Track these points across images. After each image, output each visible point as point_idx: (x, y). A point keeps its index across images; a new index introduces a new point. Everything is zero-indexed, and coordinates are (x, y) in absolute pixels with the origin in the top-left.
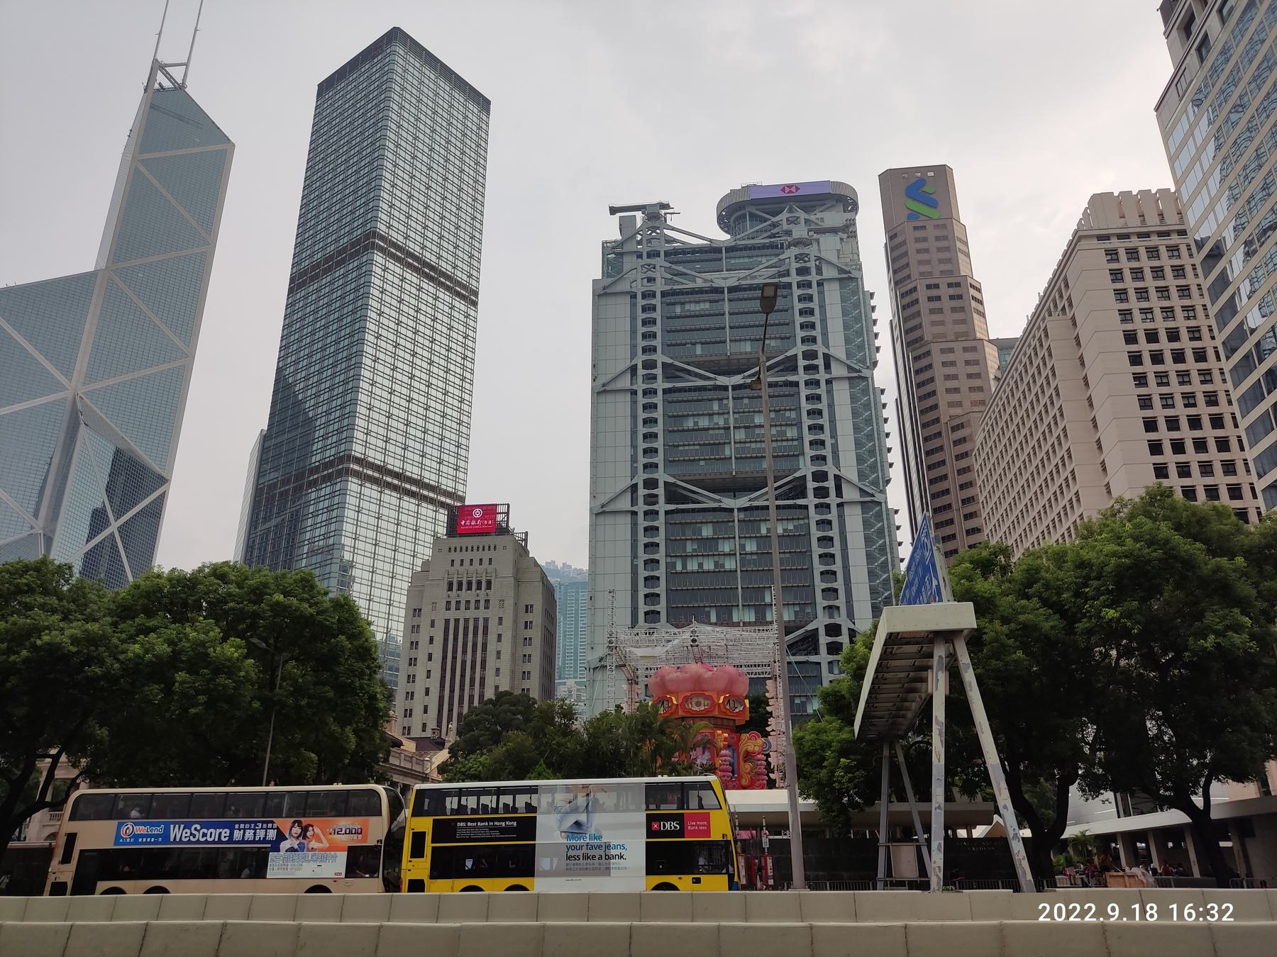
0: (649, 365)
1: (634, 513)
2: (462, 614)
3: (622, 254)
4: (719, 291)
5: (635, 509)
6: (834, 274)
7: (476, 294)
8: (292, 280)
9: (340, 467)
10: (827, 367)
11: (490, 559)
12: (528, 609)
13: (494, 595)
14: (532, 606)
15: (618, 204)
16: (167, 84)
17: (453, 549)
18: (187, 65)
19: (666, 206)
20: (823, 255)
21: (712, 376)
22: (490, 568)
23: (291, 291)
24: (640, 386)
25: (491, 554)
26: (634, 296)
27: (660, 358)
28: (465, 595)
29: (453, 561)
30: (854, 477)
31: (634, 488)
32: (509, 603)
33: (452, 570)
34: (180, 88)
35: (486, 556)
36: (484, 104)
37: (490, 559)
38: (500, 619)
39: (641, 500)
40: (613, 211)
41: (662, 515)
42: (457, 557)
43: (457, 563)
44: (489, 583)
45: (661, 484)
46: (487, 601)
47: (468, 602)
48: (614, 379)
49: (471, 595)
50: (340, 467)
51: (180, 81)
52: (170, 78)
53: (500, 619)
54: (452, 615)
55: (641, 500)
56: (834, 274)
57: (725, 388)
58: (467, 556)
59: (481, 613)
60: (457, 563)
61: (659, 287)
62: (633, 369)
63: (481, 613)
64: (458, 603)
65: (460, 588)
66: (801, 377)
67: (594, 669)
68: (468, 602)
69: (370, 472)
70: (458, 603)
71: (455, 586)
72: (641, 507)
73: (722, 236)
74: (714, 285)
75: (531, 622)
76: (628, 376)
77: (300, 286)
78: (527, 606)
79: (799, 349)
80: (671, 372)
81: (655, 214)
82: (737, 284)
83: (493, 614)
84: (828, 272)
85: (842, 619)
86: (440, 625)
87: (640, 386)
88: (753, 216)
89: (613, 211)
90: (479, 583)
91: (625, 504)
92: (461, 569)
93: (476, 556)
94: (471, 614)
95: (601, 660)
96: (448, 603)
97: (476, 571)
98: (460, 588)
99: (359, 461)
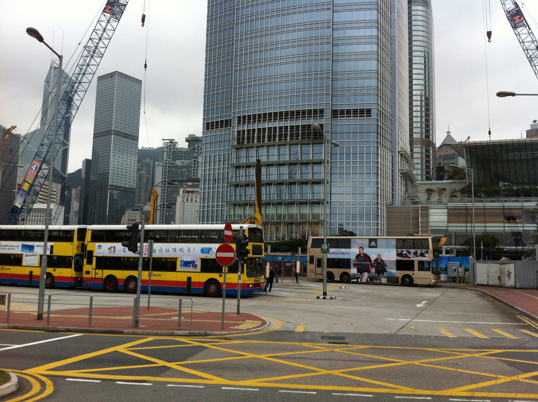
0: (165, 181)
1: (160, 210)
7: (138, 138)
8: (94, 134)
15: (164, 139)
23: (94, 137)
24: (163, 185)
25: (136, 215)
31: (161, 205)
35: (135, 215)
39: (162, 207)
42: (130, 215)
44: (135, 220)
55: (162, 207)
58: (132, 215)
61: (168, 165)
69: (114, 188)
76: (161, 183)
77: (96, 137)
87: (163, 185)
89: (163, 140)
93: (133, 215)
97: (133, 218)
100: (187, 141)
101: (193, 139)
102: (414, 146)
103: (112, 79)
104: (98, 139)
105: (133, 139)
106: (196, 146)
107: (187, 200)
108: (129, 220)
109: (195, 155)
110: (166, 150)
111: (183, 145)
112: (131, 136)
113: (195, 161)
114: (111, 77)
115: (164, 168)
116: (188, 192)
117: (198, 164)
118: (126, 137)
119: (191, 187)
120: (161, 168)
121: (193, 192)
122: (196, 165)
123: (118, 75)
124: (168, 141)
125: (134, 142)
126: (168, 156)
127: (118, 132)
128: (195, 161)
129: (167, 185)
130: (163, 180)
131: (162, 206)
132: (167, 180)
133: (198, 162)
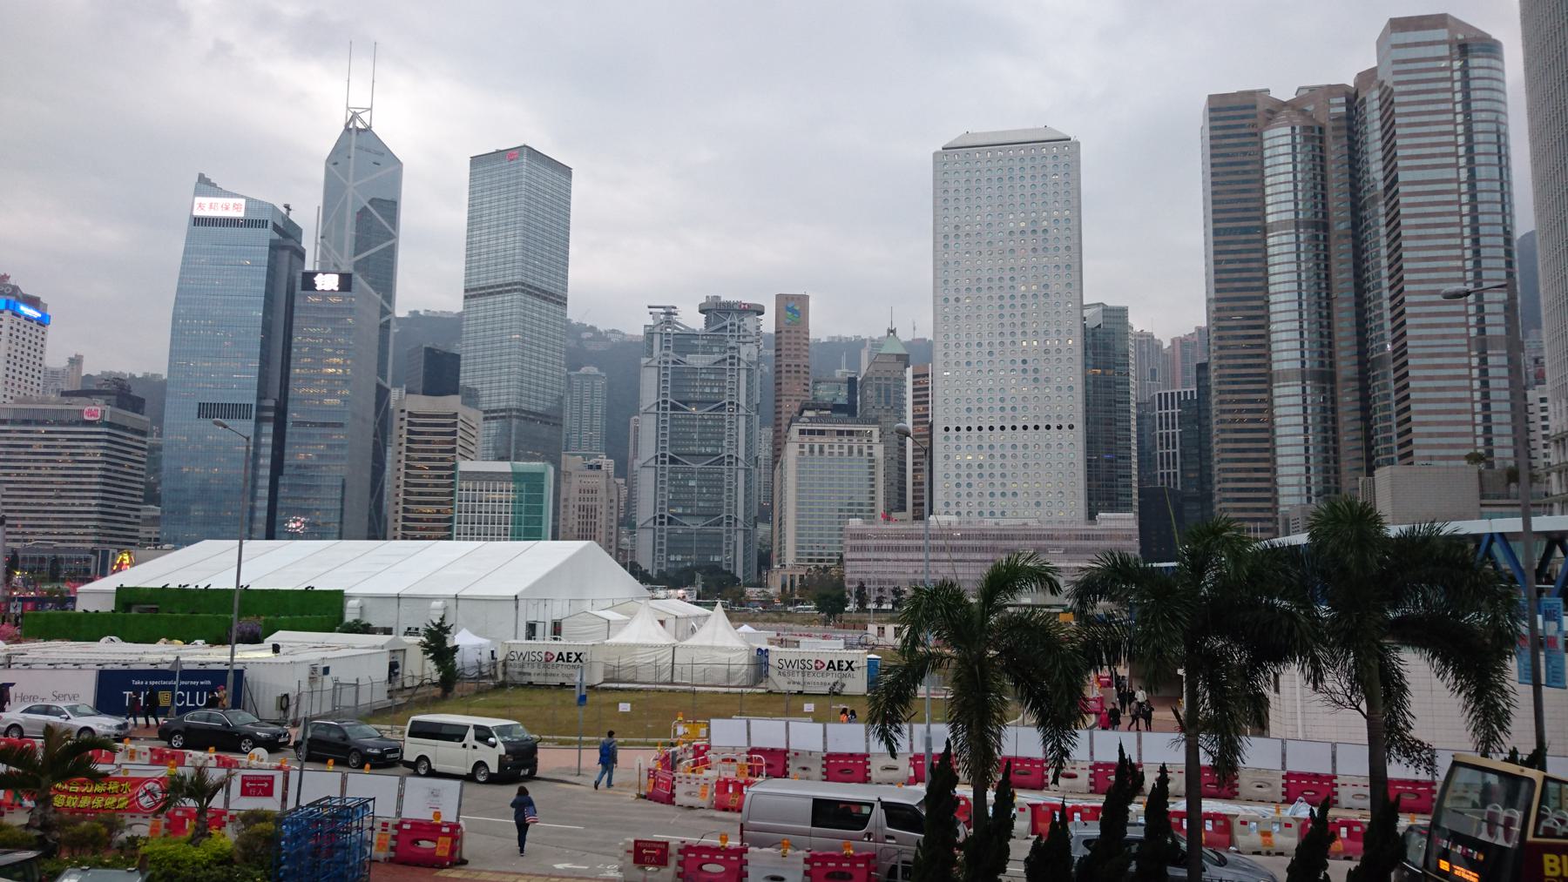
2: (586, 503)
7: (566, 299)
8: (466, 291)
10: (738, 409)
12: (611, 501)
13: (599, 495)
16: (360, 125)
18: (371, 109)
23: (466, 297)
27: (670, 399)
28: (587, 495)
30: (743, 458)
31: (657, 457)
32: (605, 500)
34: (368, 130)
36: (567, 171)
40: (650, 307)
49: (590, 495)
52: (363, 123)
54: (582, 503)
59: (594, 503)
63: (594, 503)
73: (697, 322)
76: (655, 407)
79: (726, 401)
80: (674, 407)
81: (670, 312)
84: (743, 365)
85: (733, 515)
86: (577, 506)
89: (650, 307)
94: (590, 503)
99: (518, 410)
100: (702, 311)
102: (1489, 352)
103: (512, 162)
104: (473, 302)
105: (558, 303)
106: (728, 322)
107: (812, 450)
109: (732, 343)
110: (657, 330)
111: (692, 320)
112: (553, 295)
113: (732, 357)
114: (512, 160)
115: (662, 372)
116: (811, 432)
117: (739, 365)
118: (545, 299)
119: (817, 422)
120: (654, 372)
121: (822, 433)
122: (736, 367)
123: (528, 155)
124: (662, 310)
125: (558, 308)
126: (664, 345)
127: (530, 286)
128: (732, 357)
129: (669, 412)
130: (660, 400)
131: (660, 459)
132: (670, 399)
133: (739, 359)
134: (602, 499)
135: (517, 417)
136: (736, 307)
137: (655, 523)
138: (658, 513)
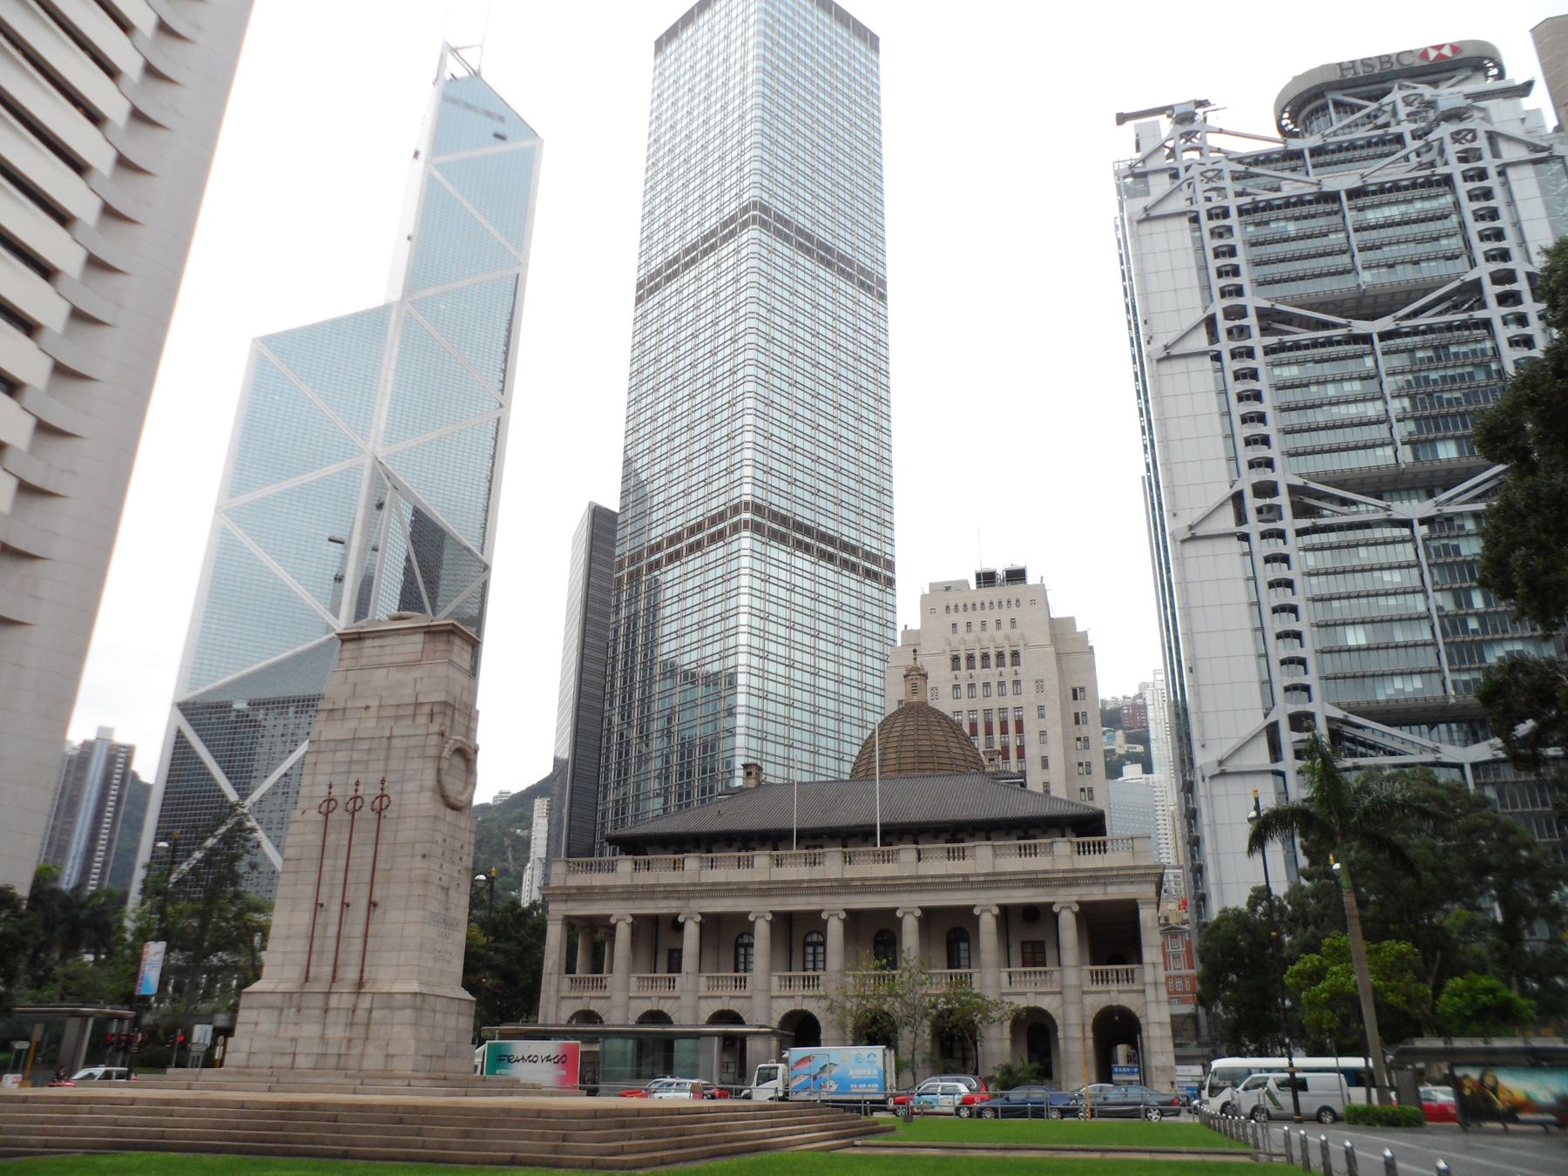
3: (1144, 175)
4: (1333, 197)
5: (1244, 529)
6: (1522, 153)
9: (736, 519)
11: (1013, 621)
13: (1027, 671)
14: (1082, 689)
15: (1127, 110)
16: (461, 73)
17: (952, 607)
18: (481, 46)
19: (1201, 104)
20: (1498, 127)
21: (1343, 321)
22: (1014, 634)
23: (639, 300)
24: (1225, 345)
25: (1014, 612)
26: (1195, 219)
27: (1252, 300)
28: (980, 674)
29: (954, 625)
31: (1238, 498)
32: (1052, 684)
33: (955, 639)
36: (872, 41)
37: (1013, 621)
38: (1041, 708)
39: (1251, 515)
40: (1122, 119)
41: (1290, 535)
42: (960, 619)
43: (962, 627)
44: (1015, 654)
45: (1283, 489)
46: (1017, 683)
47: (987, 685)
48: (1182, 338)
49: (991, 674)
50: (736, 519)
51: (475, 68)
52: (464, 63)
53: (1041, 708)
56: (1522, 153)
57: (1366, 339)
59: (1010, 701)
60: (962, 627)
61: (1232, 203)
62: (1210, 322)
64: (971, 686)
65: (971, 666)
66: (1494, 312)
67: (1212, 777)
68: (987, 685)
70: (971, 686)
71: (963, 663)
72: (1254, 526)
74: (1325, 189)
75: (1085, 714)
76: (1203, 332)
78: (1075, 691)
79: (1484, 270)
82: (1359, 184)
83: (1028, 698)
87: (1225, 345)
88: (1338, 105)
89: (1122, 119)
90: (1000, 656)
91: (1226, 520)
92: (969, 637)
93: (990, 616)
94: (994, 702)
95: (1220, 763)
96: (956, 687)
97: (995, 640)
98: (971, 666)
101: (1350, 75)
108: (956, 659)
117: (1496, 154)
134: (1040, 685)
135: (757, 528)
136: (1407, 61)
137: (1275, 751)
138: (1281, 715)
